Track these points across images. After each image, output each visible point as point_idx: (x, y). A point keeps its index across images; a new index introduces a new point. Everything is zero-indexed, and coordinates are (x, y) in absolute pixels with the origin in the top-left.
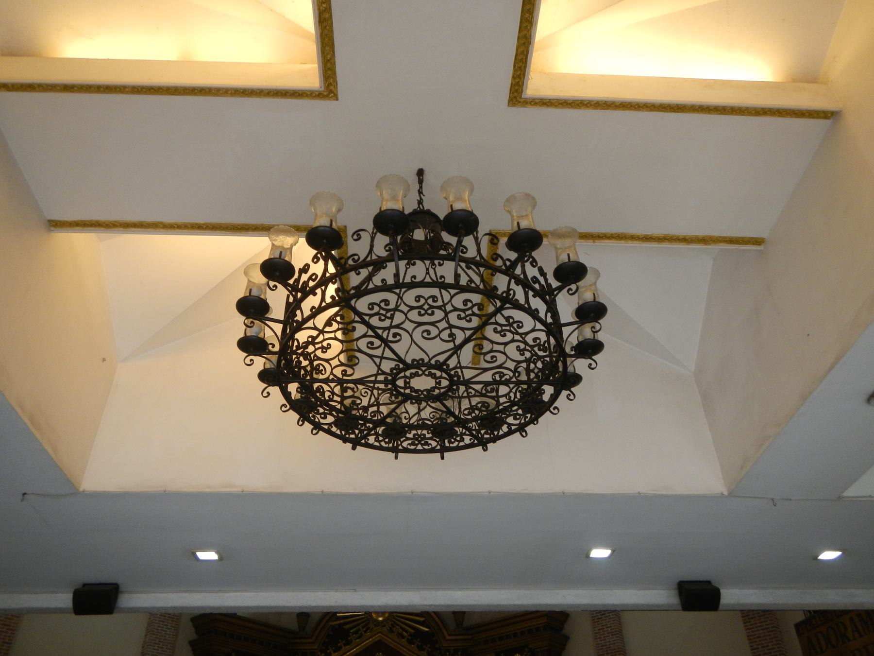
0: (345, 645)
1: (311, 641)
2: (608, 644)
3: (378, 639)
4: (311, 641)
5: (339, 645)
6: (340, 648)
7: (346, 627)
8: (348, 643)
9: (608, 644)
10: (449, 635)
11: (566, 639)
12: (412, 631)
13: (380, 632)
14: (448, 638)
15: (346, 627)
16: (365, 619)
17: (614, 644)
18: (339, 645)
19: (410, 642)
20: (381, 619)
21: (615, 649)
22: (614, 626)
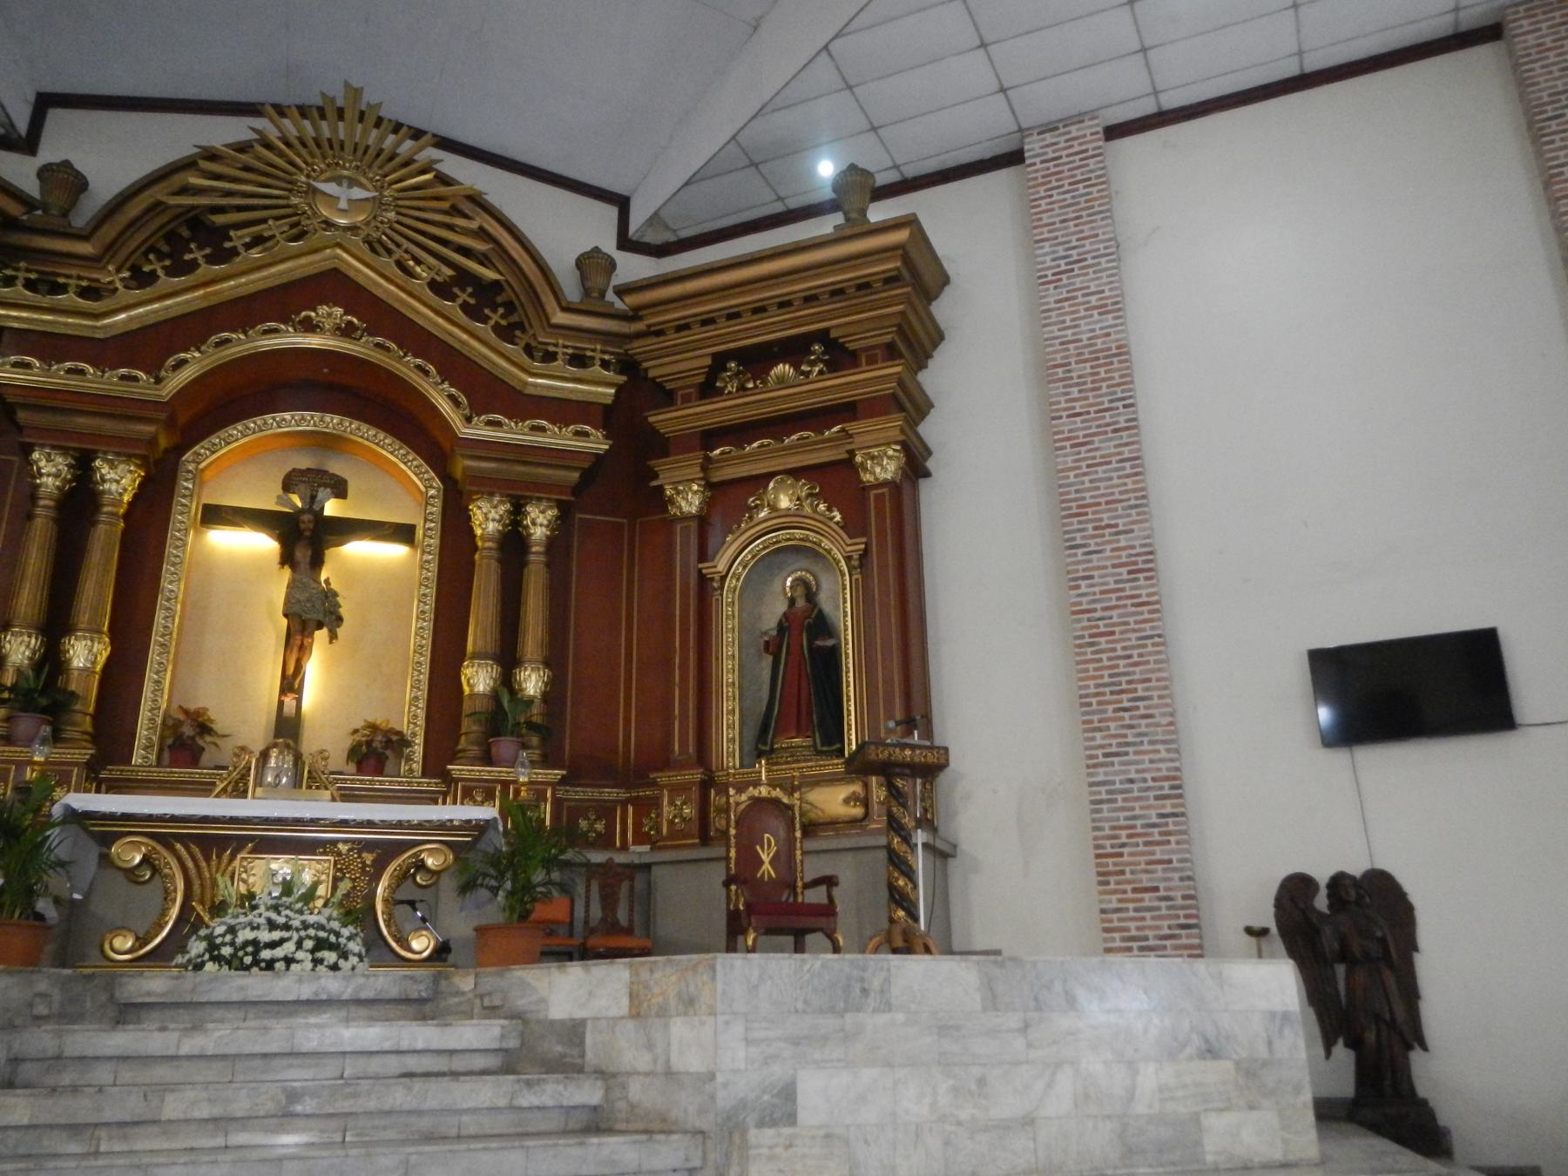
0: (211, 260)
1: (85, 248)
2: (1084, 337)
3: (328, 265)
4: (85, 248)
5: (188, 257)
6: (193, 265)
7: (220, 219)
8: (222, 255)
9: (1084, 337)
10: (567, 309)
11: (938, 337)
12: (450, 272)
13: (339, 245)
14: (560, 318)
15: (220, 219)
16: (289, 211)
17: (1108, 335)
18: (188, 257)
19: (438, 288)
20: (343, 221)
21: (1110, 349)
22: (1111, 290)
